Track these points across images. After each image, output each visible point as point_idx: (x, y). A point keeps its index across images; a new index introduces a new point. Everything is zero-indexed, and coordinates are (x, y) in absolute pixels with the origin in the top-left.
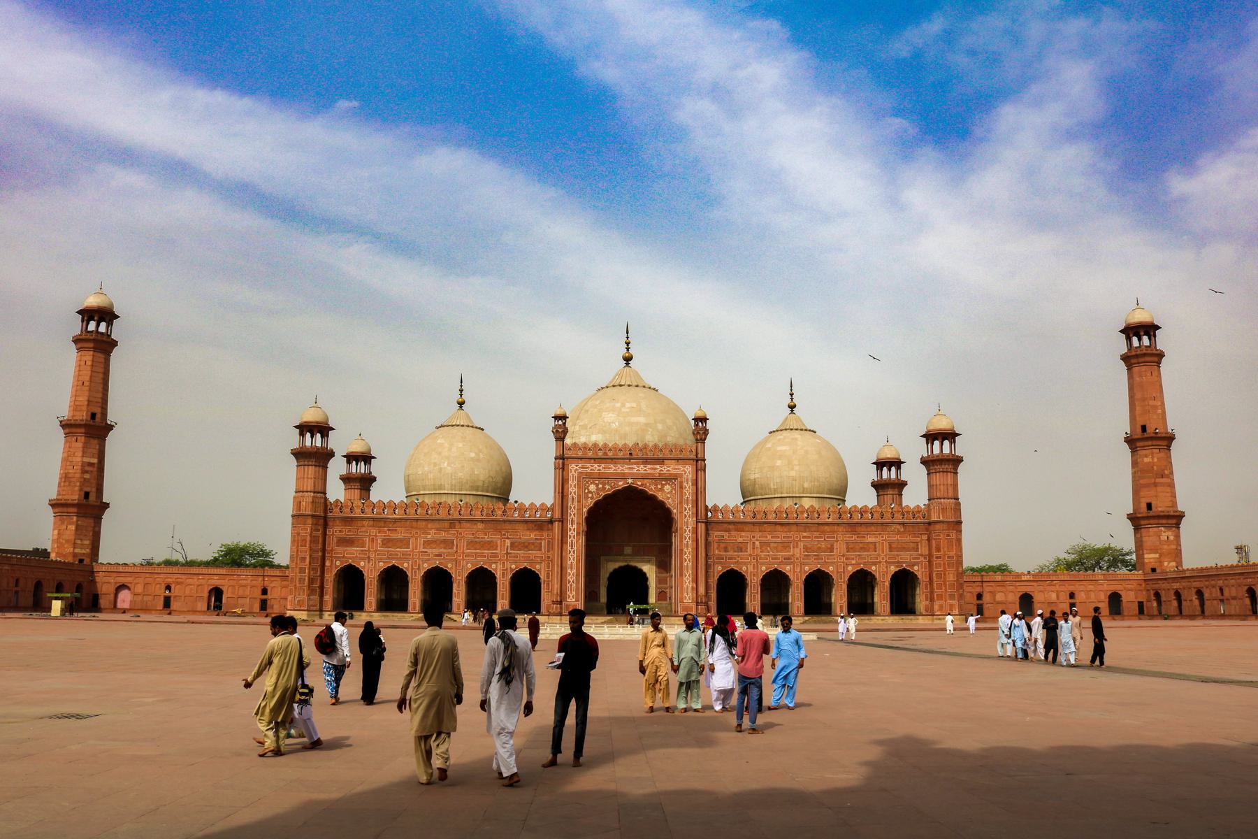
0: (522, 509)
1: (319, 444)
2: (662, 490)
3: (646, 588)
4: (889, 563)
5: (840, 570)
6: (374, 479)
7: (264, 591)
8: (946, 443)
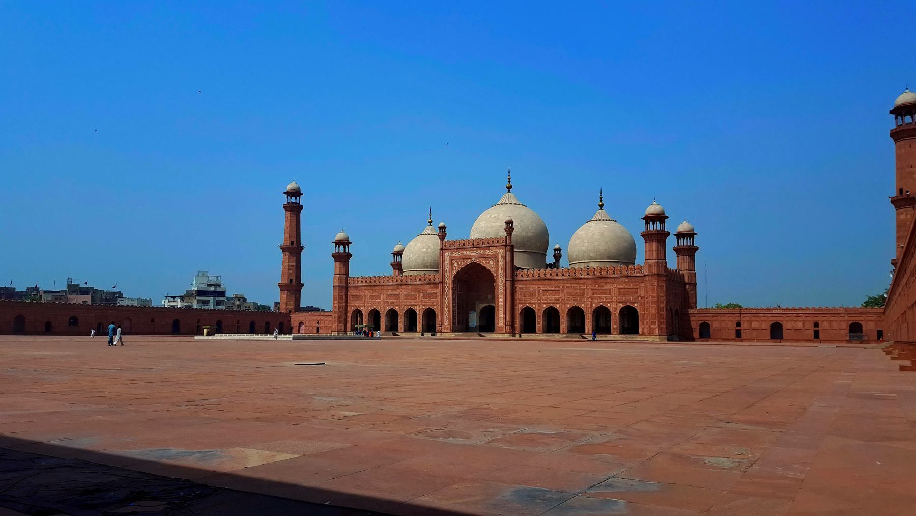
5: (588, 307)
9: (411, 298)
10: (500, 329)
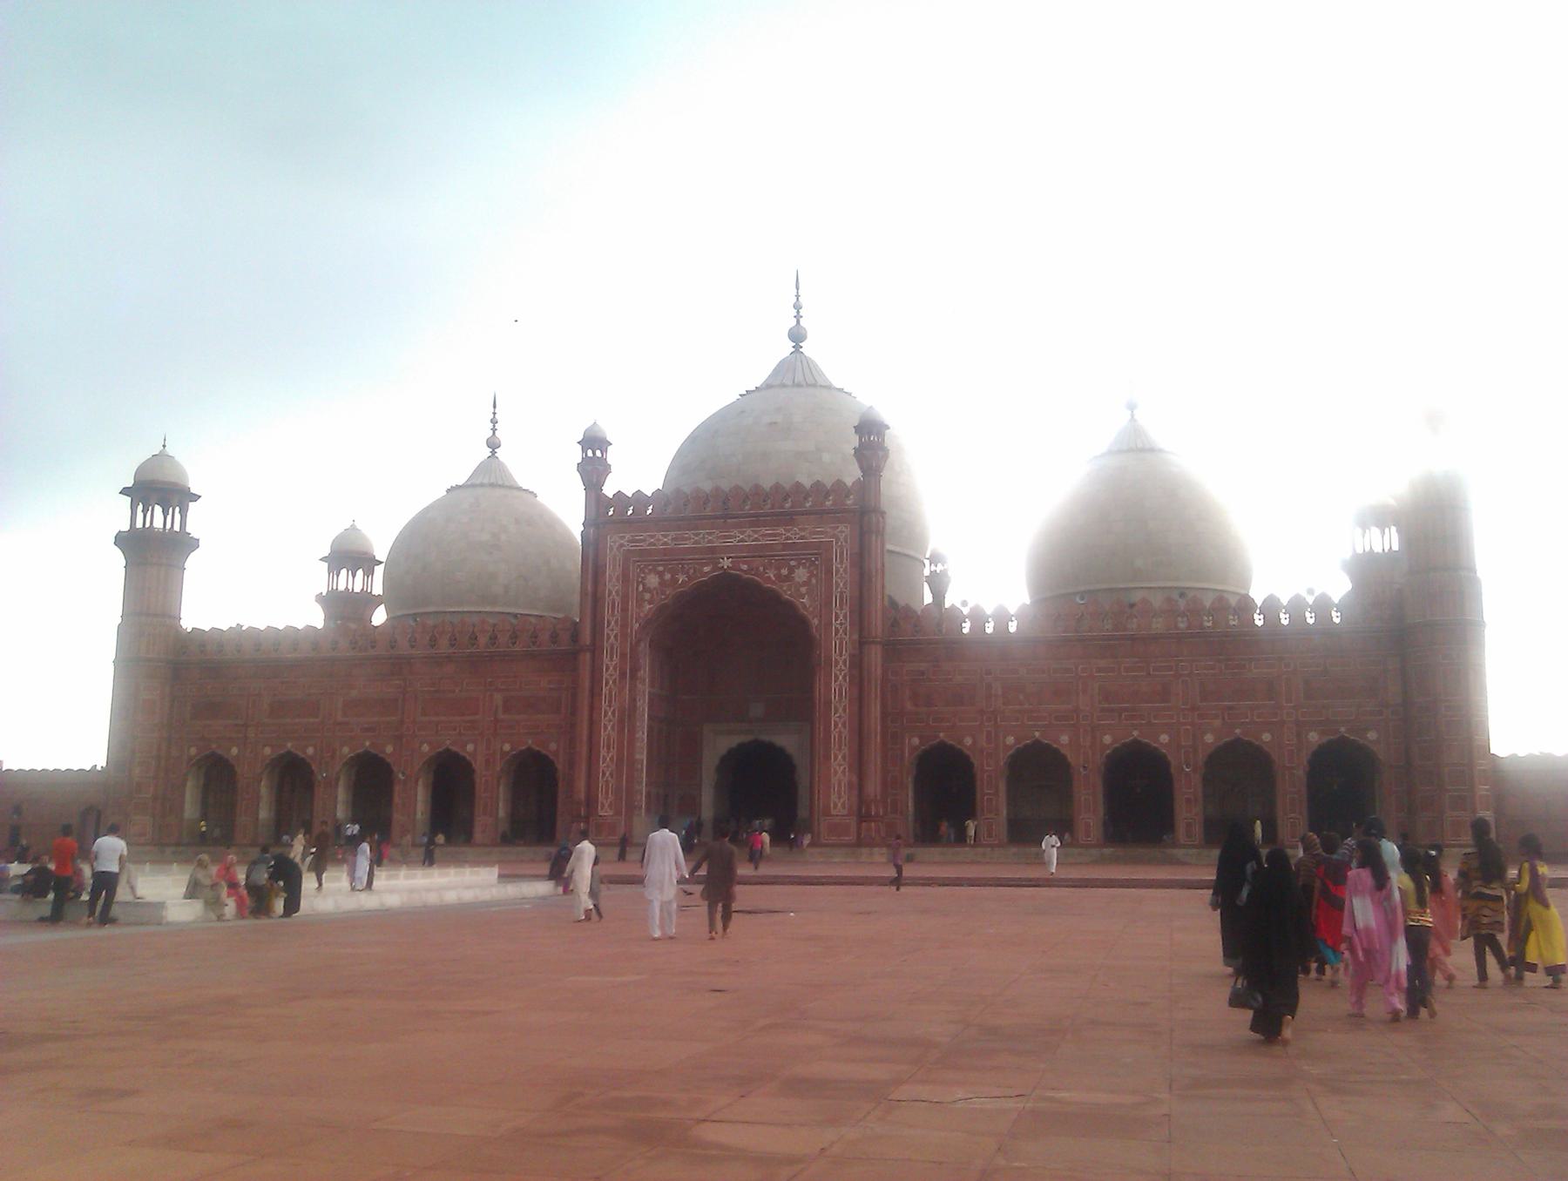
2: (788, 578)
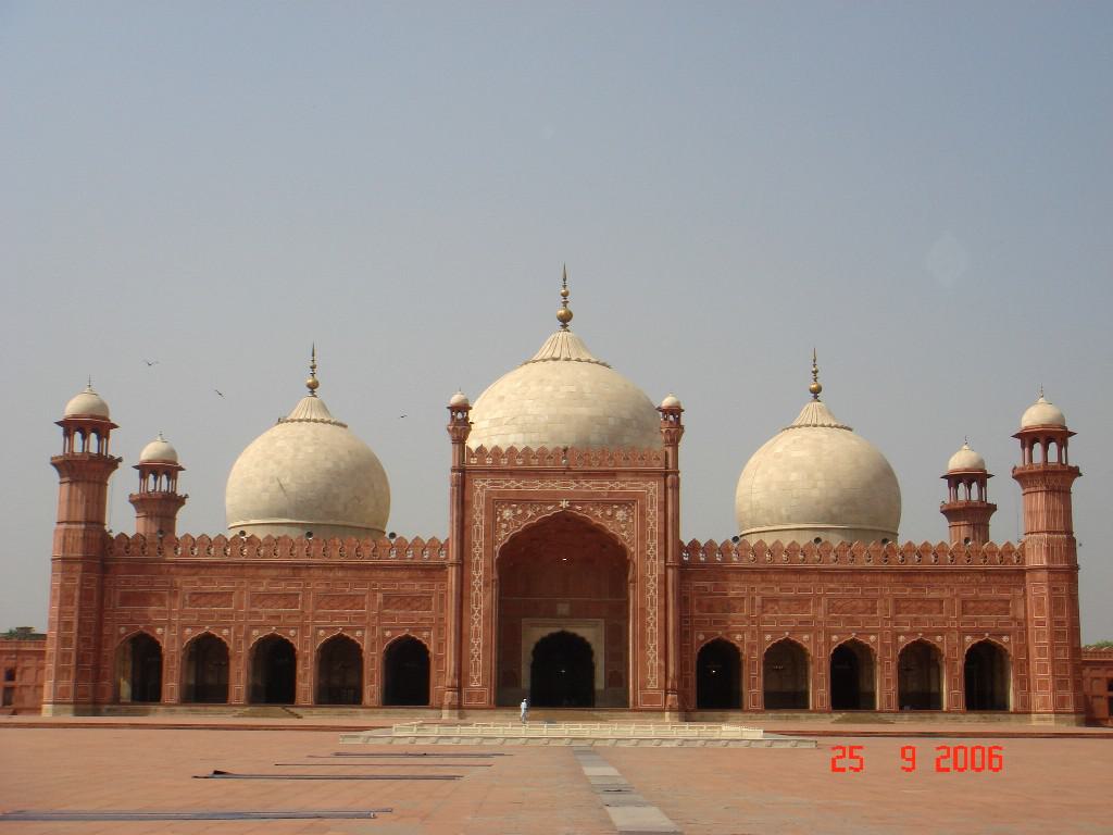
0: (402, 546)
1: (94, 449)
2: (612, 517)
3: (591, 668)
4: (964, 633)
5: (885, 640)
6: (181, 501)
7: (11, 675)
8: (1053, 447)
9: (341, 605)
10: (650, 699)
